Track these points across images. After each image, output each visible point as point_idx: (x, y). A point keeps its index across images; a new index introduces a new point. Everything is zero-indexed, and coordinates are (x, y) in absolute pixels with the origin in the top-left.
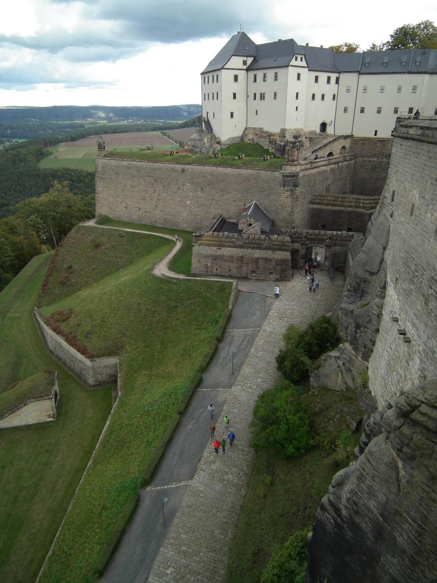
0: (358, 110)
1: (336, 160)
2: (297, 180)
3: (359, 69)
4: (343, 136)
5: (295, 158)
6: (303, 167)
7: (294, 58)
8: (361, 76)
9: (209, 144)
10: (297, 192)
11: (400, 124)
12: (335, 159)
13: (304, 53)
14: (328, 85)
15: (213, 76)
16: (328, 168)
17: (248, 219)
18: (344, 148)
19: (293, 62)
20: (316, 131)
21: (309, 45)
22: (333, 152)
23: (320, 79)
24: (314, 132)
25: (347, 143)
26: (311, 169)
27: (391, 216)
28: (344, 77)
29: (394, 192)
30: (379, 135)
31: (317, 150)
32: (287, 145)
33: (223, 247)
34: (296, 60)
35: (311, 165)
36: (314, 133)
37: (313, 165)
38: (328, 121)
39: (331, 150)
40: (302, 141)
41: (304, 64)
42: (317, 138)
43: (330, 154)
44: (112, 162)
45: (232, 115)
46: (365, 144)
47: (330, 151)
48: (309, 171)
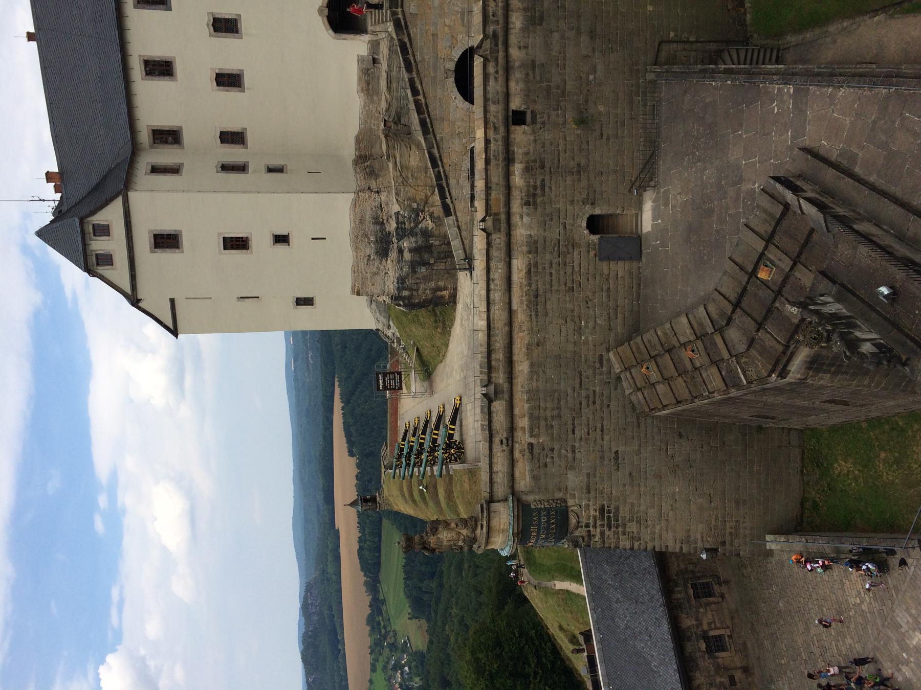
1: (493, 146)
2: (544, 519)
10: (584, 521)
13: (77, 220)
16: (521, 233)
20: (361, 60)
21: (32, 30)
22: (457, 54)
31: (438, 177)
32: (410, 297)
34: (106, 259)
37: (500, 378)
40: (397, 213)
41: (112, 214)
42: (389, 88)
45: (305, 302)
47: (452, 80)
48: (517, 411)
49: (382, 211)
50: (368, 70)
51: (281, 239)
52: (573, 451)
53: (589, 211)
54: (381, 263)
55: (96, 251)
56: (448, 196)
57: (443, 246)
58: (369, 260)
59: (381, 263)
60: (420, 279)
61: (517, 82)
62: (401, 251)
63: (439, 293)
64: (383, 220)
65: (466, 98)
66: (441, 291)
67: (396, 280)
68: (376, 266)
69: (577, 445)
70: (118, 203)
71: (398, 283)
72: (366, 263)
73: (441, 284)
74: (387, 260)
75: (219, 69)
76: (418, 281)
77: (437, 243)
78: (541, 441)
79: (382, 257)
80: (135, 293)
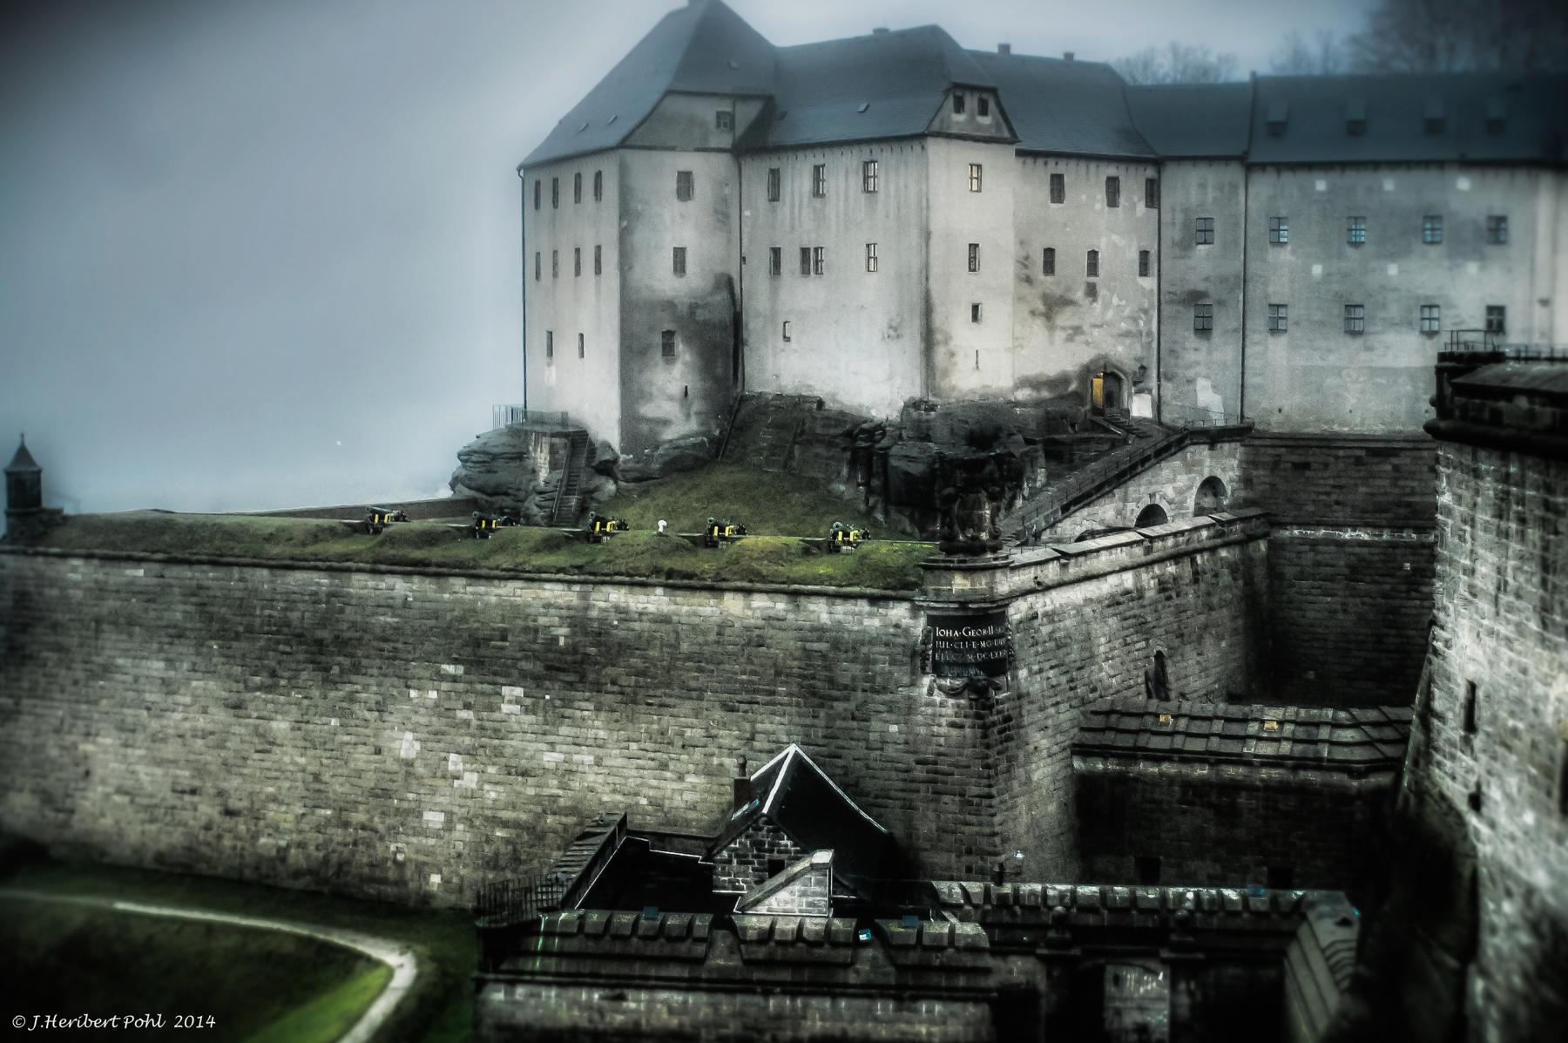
2: (1002, 642)
5: (984, 536)
6: (1023, 579)
9: (559, 474)
11: (1459, 380)
12: (1175, 534)
15: (578, 176)
16: (1148, 580)
17: (764, 835)
18: (1212, 485)
22: (1164, 505)
26: (1061, 584)
27: (1476, 801)
29: (1472, 687)
33: (639, 988)
35: (1064, 566)
43: (1151, 515)
44: (74, 569)
52: (1041, 671)
53: (1165, 650)
65: (1139, 519)
69: (1044, 675)
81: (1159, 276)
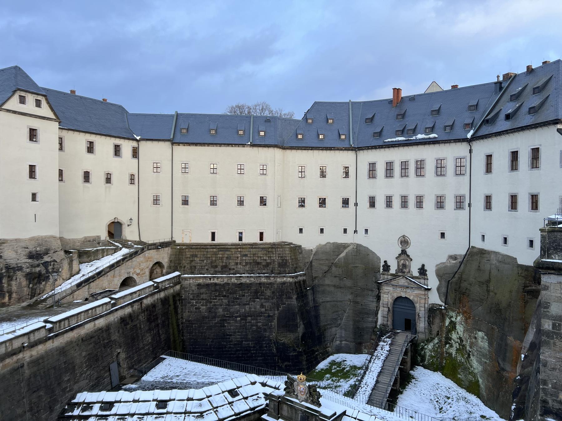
0: (178, 200)
3: (172, 137)
4: (154, 244)
7: (16, 98)
8: (176, 148)
14: (117, 159)
19: (13, 103)
20: (99, 237)
22: (135, 276)
23: (97, 147)
24: (94, 240)
25: (164, 256)
28: (146, 148)
30: (218, 241)
34: (22, 100)
36: (96, 241)
38: (124, 219)
39: (129, 273)
40: (55, 261)
41: (45, 111)
46: (196, 256)
47: (126, 276)
49: (54, 252)
50: (95, 241)
51: (34, 197)
54: (24, 255)
55: (28, 97)
56: (85, 284)
57: (39, 291)
58: (25, 248)
59: (24, 255)
60: (20, 280)
61: (150, 301)
62: (38, 266)
63: (7, 295)
64: (49, 254)
66: (9, 296)
67: (19, 265)
68: (22, 252)
70: (51, 115)
71: (18, 267)
72: (23, 246)
73: (14, 295)
74: (27, 259)
75: (91, 174)
76: (18, 280)
77: (42, 286)
78: (26, 371)
79: (28, 256)
80: (5, 111)
81: (139, 185)
